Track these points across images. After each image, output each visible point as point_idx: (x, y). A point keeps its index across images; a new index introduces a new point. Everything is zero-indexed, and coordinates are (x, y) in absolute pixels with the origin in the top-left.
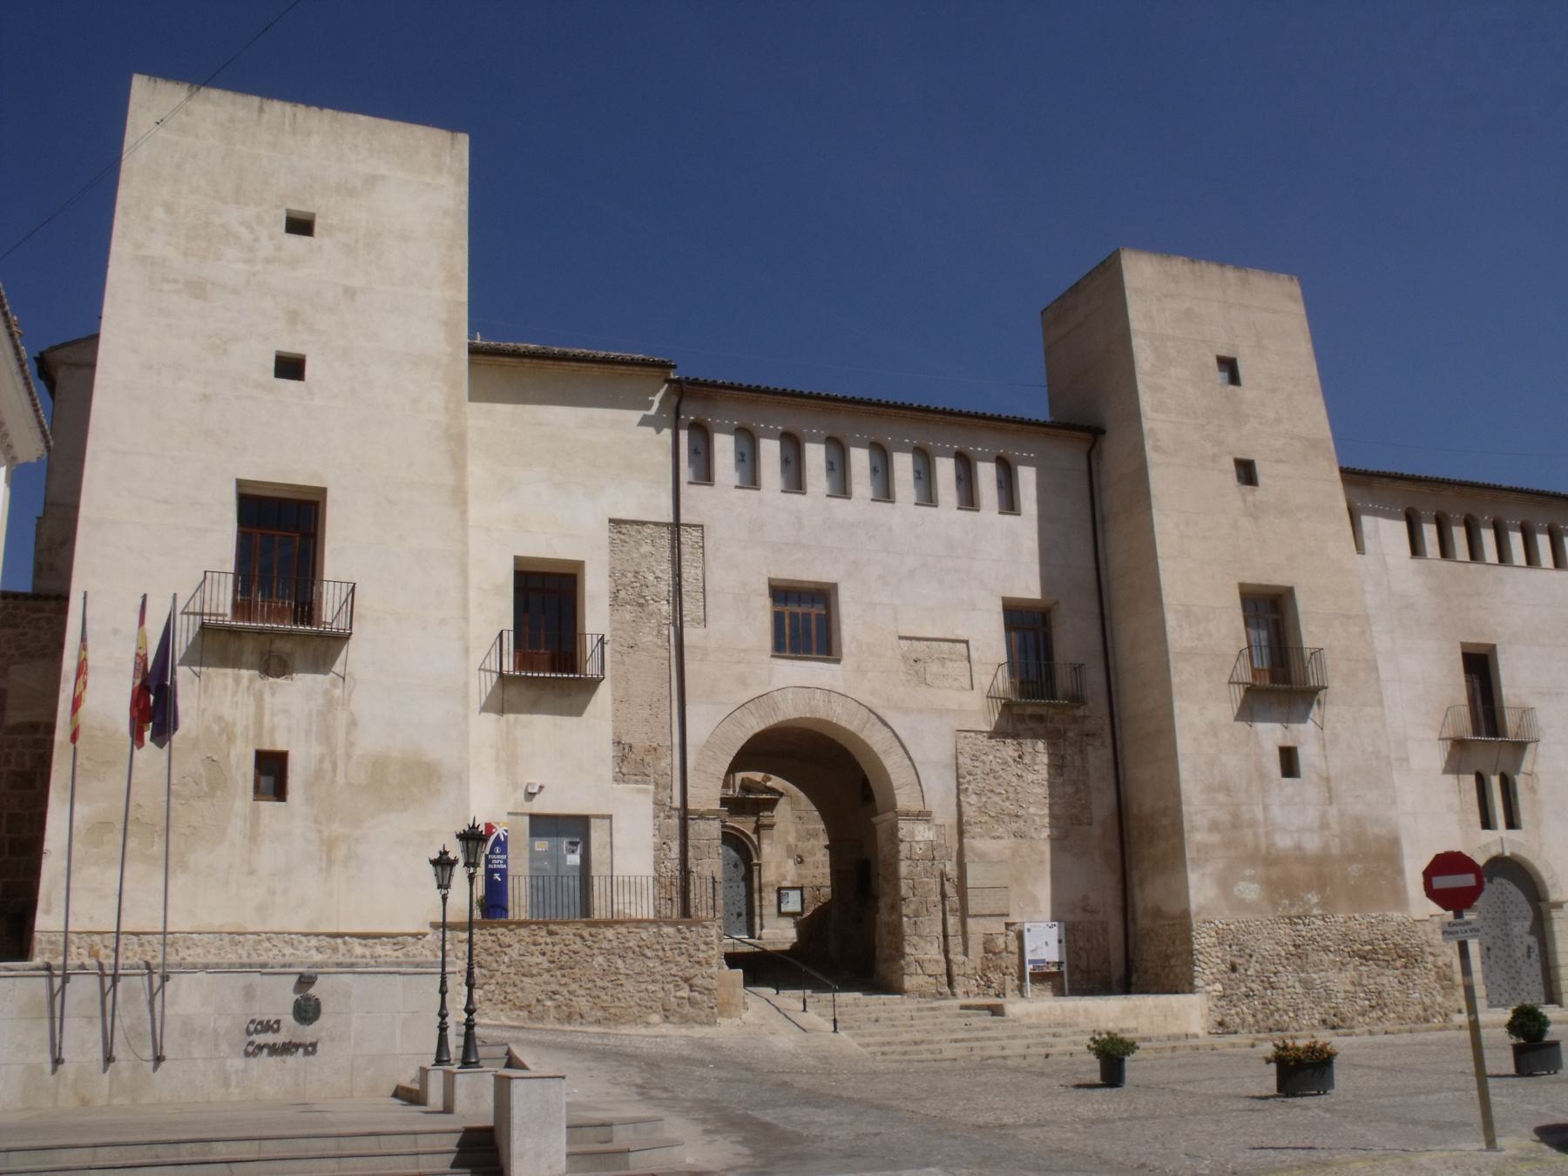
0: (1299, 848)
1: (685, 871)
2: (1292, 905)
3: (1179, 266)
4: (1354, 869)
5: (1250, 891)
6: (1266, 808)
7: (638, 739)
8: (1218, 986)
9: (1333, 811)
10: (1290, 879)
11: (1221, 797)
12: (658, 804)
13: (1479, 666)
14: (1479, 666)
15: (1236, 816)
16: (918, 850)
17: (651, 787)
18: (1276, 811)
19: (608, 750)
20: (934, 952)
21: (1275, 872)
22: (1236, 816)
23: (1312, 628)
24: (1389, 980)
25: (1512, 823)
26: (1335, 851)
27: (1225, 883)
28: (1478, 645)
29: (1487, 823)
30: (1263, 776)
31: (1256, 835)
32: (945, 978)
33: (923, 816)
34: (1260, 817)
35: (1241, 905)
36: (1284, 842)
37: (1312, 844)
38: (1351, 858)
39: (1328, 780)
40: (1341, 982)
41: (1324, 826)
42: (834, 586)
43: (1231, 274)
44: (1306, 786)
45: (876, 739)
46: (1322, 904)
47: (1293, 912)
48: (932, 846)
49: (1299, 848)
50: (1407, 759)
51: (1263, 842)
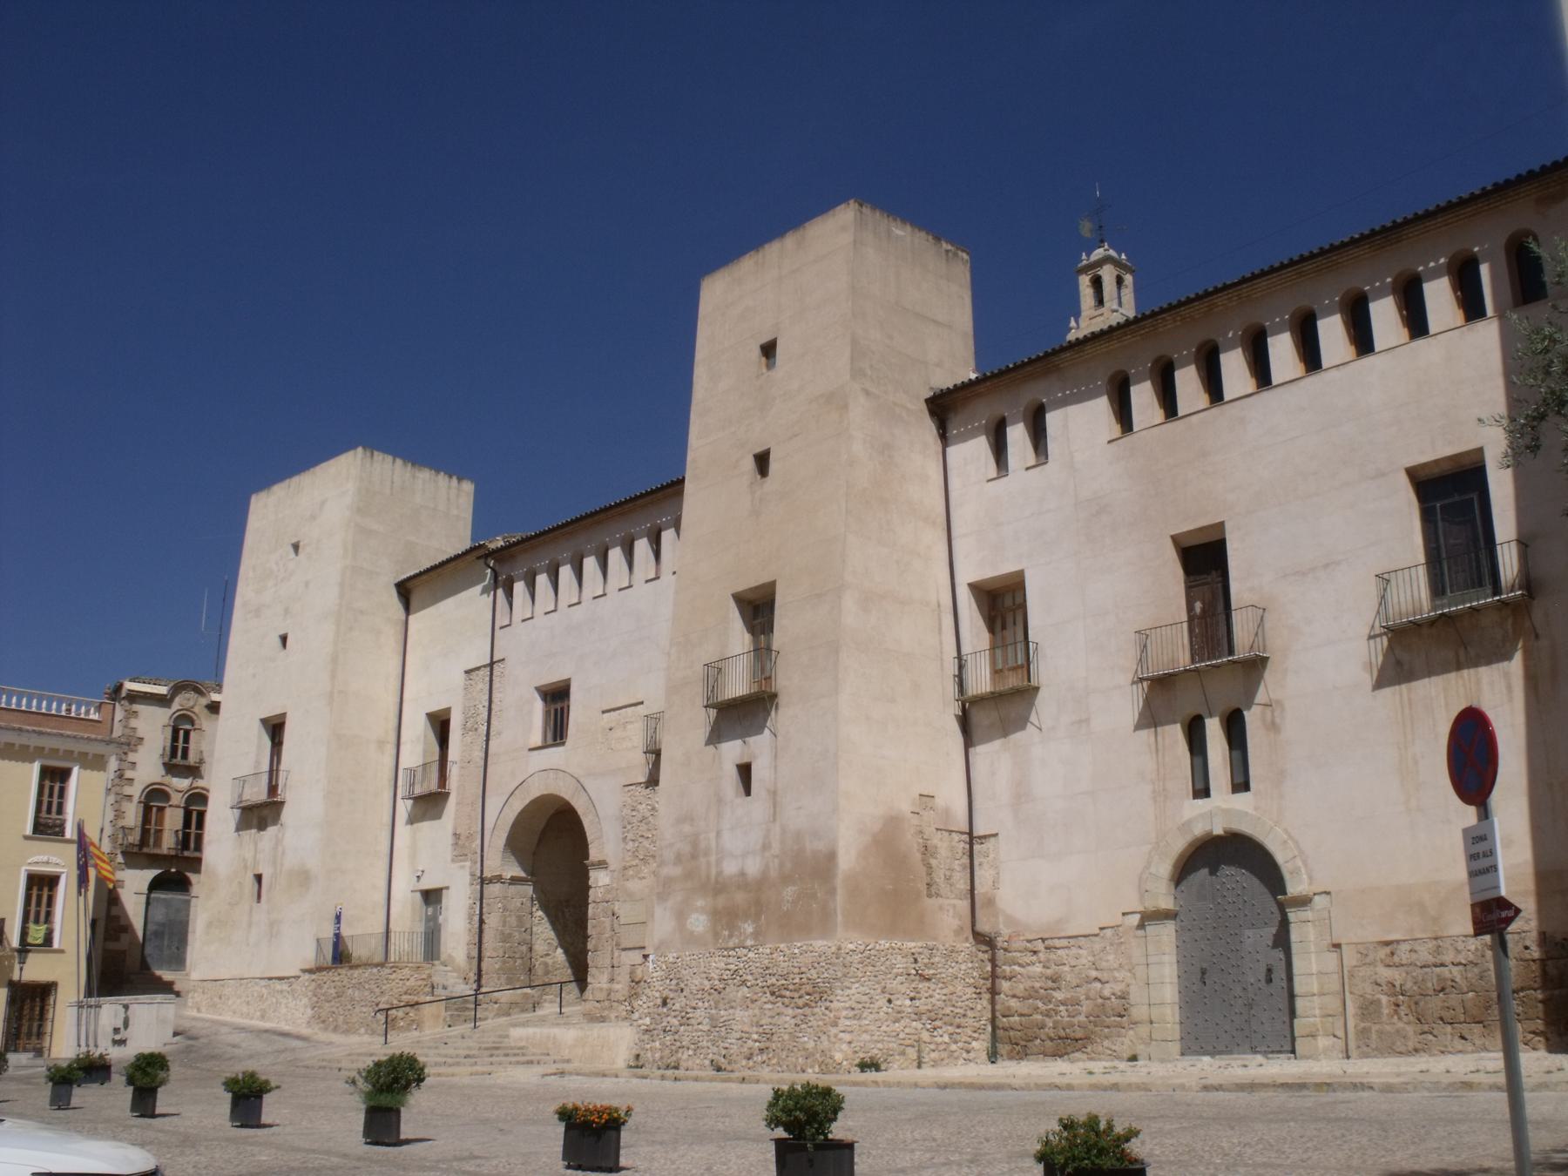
0: (742, 874)
1: (482, 922)
2: (731, 936)
3: (747, 264)
4: (789, 892)
5: (699, 923)
6: (718, 834)
8: (647, 1021)
10: (741, 907)
11: (687, 828)
12: (472, 875)
13: (1204, 559)
14: (1204, 559)
15: (695, 844)
17: (468, 864)
18: (726, 835)
19: (450, 840)
21: (721, 901)
24: (788, 1018)
25: (1241, 784)
26: (773, 874)
27: (681, 916)
28: (1201, 529)
31: (708, 863)
33: (602, 865)
34: (713, 844)
35: (690, 939)
36: (730, 868)
37: (753, 867)
38: (786, 879)
39: (775, 793)
40: (741, 1018)
41: (766, 847)
43: (790, 240)
44: (757, 805)
46: (756, 935)
47: (731, 944)
49: (742, 874)
50: (1087, 721)
51: (713, 872)
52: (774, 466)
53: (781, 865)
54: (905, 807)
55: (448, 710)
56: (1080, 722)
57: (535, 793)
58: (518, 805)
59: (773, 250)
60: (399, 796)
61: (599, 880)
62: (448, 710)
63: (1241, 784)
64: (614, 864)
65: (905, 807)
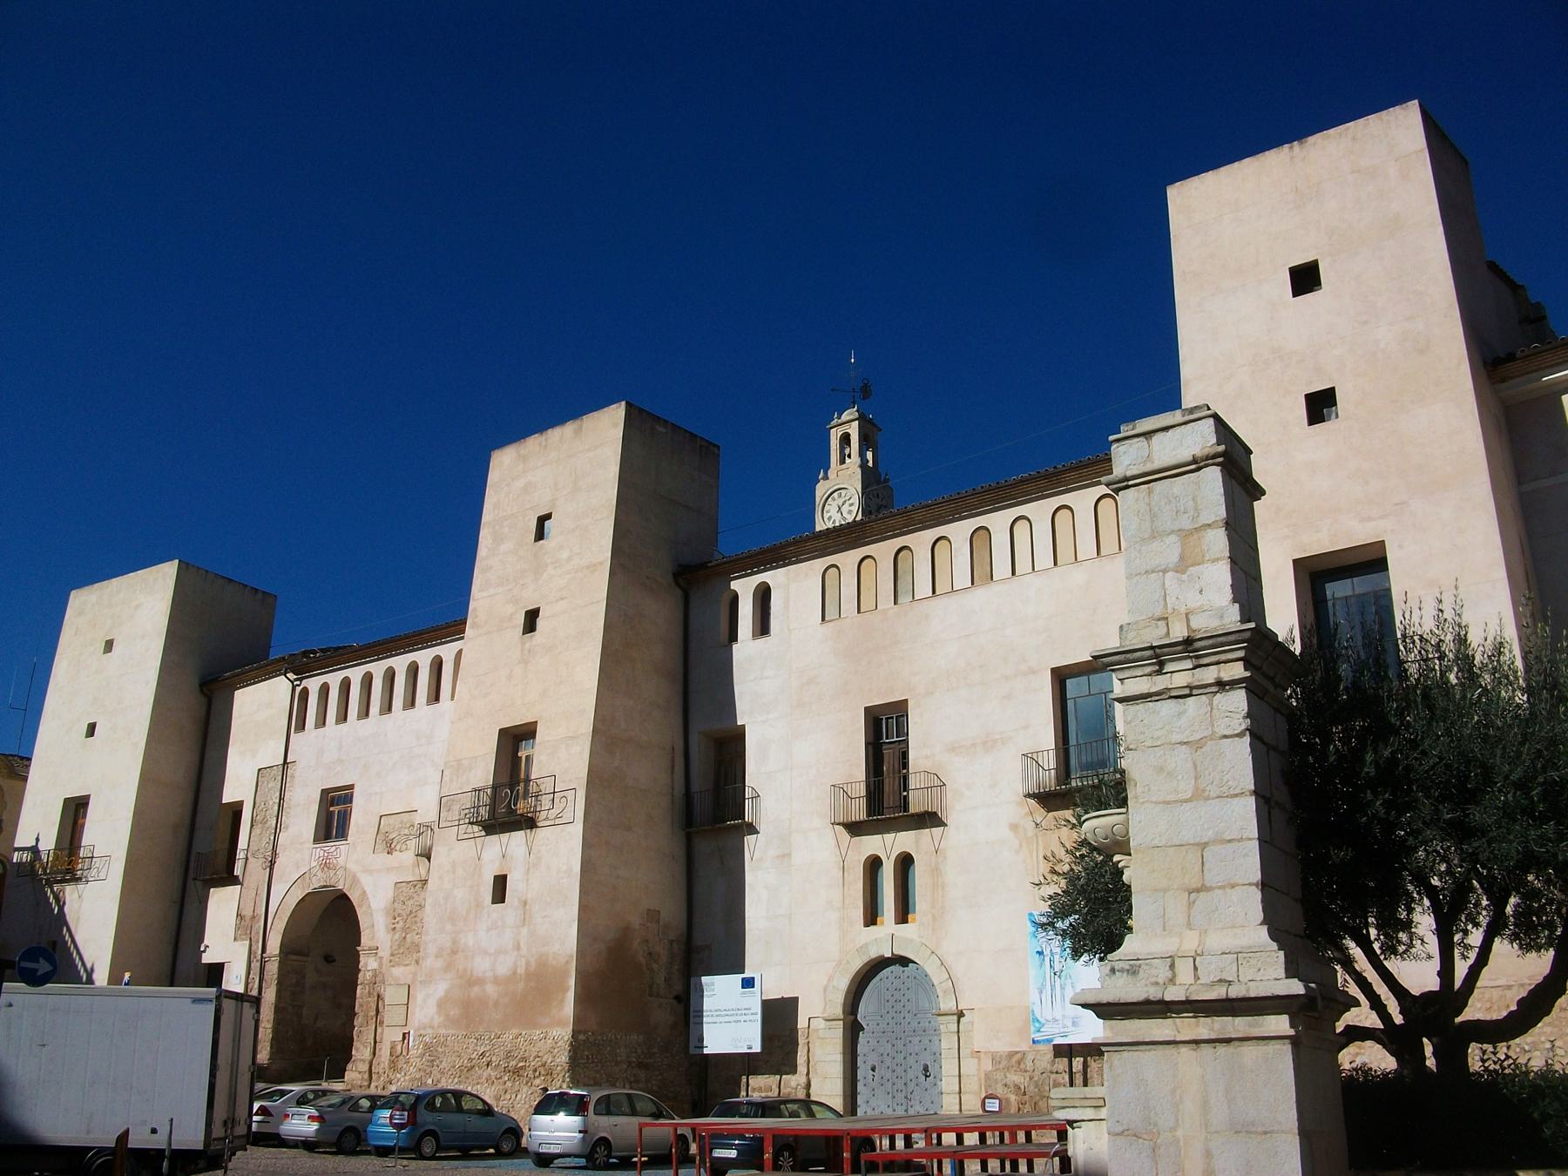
3: (533, 443)
7: (248, 912)
9: (524, 931)
11: (449, 927)
15: (455, 942)
16: (369, 975)
20: (367, 1053)
22: (455, 942)
23: (543, 758)
29: (872, 917)
30: (479, 905)
32: (366, 1076)
39: (525, 903)
42: (351, 787)
43: (569, 429)
45: (354, 897)
48: (375, 973)
52: (541, 623)
53: (528, 964)
54: (636, 921)
55: (241, 803)
56: (783, 856)
57: (315, 884)
58: (297, 894)
59: (555, 434)
60: (191, 875)
61: (368, 964)
62: (241, 803)
63: (903, 914)
64: (384, 953)
65: (636, 921)
